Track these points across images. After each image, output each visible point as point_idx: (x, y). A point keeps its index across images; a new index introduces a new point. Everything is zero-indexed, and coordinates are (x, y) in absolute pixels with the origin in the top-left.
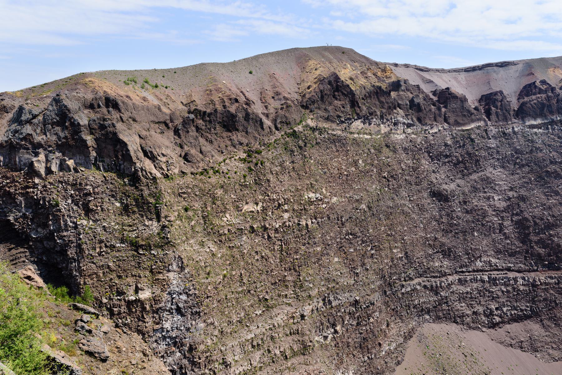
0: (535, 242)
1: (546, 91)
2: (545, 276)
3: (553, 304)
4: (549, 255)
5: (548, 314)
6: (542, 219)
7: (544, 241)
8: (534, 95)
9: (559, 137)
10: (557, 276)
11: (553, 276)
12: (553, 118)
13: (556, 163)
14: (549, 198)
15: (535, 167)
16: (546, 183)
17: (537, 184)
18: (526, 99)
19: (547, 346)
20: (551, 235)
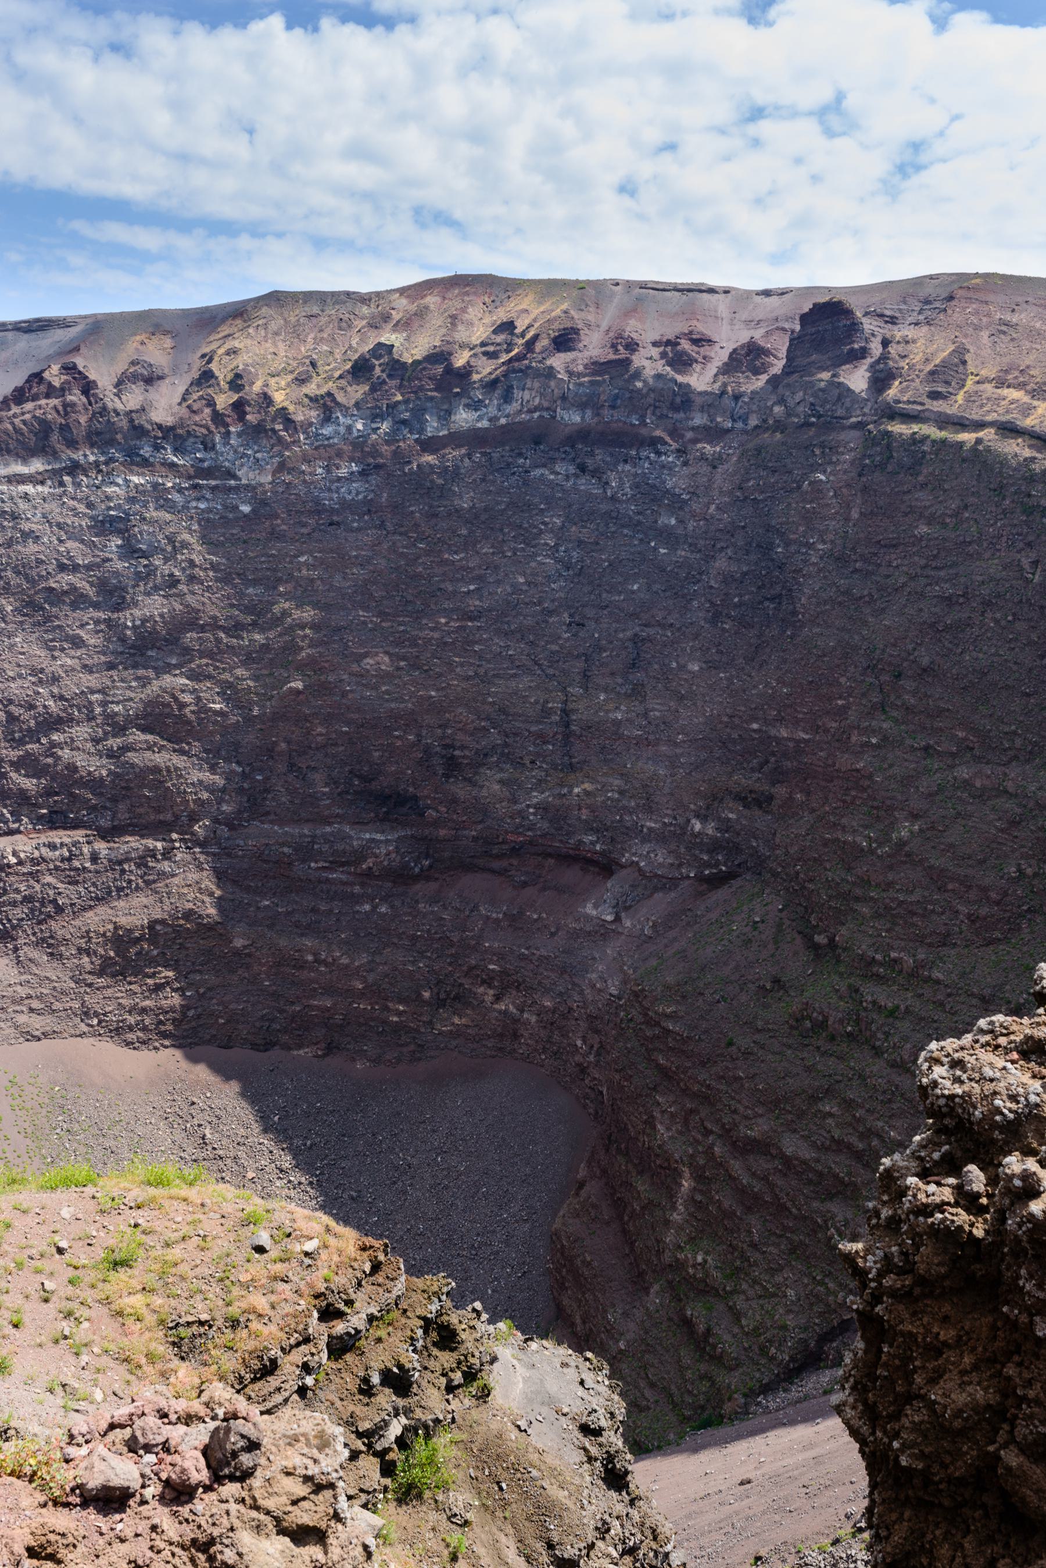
0: (12, 764)
1: (62, 391)
2: (34, 843)
3: (50, 909)
4: (49, 792)
5: (34, 934)
6: (32, 707)
7: (37, 760)
8: (33, 400)
9: (90, 506)
10: (67, 840)
11: (58, 841)
12: (75, 456)
13: (75, 568)
14: (56, 654)
15: (15, 580)
16: (48, 619)
17: (22, 623)
18: (15, 409)
19: (18, 1008)
20: (53, 745)
